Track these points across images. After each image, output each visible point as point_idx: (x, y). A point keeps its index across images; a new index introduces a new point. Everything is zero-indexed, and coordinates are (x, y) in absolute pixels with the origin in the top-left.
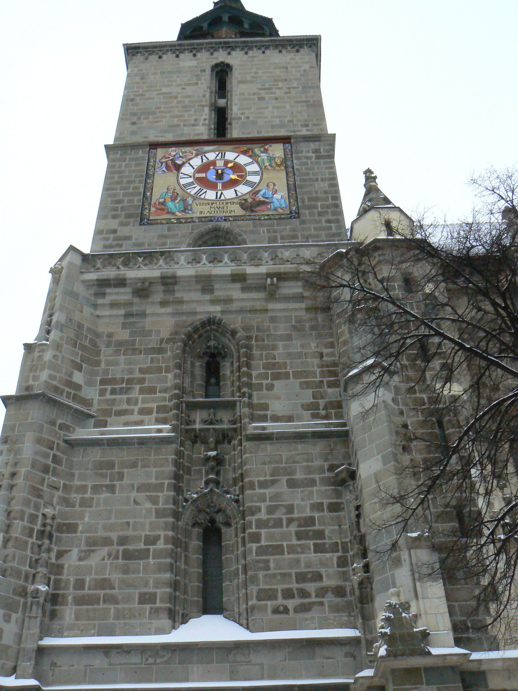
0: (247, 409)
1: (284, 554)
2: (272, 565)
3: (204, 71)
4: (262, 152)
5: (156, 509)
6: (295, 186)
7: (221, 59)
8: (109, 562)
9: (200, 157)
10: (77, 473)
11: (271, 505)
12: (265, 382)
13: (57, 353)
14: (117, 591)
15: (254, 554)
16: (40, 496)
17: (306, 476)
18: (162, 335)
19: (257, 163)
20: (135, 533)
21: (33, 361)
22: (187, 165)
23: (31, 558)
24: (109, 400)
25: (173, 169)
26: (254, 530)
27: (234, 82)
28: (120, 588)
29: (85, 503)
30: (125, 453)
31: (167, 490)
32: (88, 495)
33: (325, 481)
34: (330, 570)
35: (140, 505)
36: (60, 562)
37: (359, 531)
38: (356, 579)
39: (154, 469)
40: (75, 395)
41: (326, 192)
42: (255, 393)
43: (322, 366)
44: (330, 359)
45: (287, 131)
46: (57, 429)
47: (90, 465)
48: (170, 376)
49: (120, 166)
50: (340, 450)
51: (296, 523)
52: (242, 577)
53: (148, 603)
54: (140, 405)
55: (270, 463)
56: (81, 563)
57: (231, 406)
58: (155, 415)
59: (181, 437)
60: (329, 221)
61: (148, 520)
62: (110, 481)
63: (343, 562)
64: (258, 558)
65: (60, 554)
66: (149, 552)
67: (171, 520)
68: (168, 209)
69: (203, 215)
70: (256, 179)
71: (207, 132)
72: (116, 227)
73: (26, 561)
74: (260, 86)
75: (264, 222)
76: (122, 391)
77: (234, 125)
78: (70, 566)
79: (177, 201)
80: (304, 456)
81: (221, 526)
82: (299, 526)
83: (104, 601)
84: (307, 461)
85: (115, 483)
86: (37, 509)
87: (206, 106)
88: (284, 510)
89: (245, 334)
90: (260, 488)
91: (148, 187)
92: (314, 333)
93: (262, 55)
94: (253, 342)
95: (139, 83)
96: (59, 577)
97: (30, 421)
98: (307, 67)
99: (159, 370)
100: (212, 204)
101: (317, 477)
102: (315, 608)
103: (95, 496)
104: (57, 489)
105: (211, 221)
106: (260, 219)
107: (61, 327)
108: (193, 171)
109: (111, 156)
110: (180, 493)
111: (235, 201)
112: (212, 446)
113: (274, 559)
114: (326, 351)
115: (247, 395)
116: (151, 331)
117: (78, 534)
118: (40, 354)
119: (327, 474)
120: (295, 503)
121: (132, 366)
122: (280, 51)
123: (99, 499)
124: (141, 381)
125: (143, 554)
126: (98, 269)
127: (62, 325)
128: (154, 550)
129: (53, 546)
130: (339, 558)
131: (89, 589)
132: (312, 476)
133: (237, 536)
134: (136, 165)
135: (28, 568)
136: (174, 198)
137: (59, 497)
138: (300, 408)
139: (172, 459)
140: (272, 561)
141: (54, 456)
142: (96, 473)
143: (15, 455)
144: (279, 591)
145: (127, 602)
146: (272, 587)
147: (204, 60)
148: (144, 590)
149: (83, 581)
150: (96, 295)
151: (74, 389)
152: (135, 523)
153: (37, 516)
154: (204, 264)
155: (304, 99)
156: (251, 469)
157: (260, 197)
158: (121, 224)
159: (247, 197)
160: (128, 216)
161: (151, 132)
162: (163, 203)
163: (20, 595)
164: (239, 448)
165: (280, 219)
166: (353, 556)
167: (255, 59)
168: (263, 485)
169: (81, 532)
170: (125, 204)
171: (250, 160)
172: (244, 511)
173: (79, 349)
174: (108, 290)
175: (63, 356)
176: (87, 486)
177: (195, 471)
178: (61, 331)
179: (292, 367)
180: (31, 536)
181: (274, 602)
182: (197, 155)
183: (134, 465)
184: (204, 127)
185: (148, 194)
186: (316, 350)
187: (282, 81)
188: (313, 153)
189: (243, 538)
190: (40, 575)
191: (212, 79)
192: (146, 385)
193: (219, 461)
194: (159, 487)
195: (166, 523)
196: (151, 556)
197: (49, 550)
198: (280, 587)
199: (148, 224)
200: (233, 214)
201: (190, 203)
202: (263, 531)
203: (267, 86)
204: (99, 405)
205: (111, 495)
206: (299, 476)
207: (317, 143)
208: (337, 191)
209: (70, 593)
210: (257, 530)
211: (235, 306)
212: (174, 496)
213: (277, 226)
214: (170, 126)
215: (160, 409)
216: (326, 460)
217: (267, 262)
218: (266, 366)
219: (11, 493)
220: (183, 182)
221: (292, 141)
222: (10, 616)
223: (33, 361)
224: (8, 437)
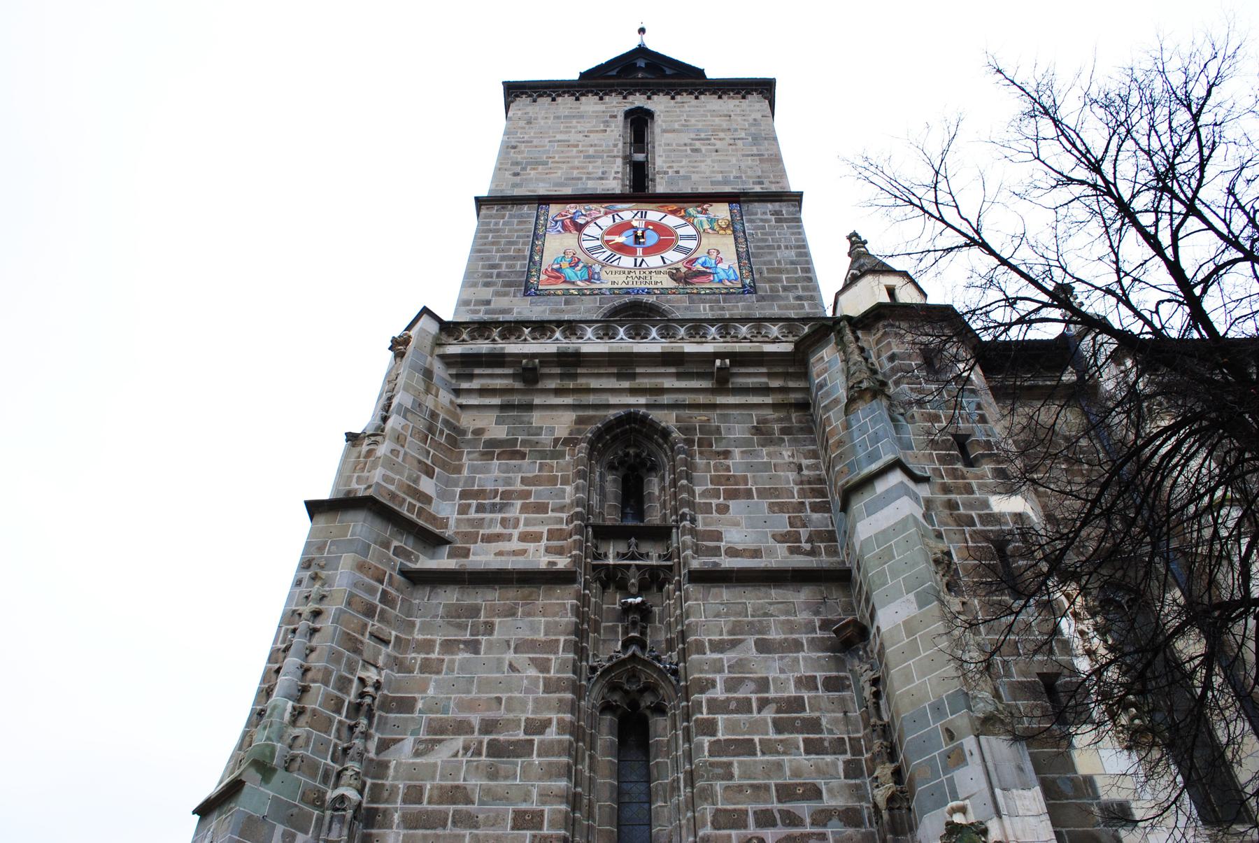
0: (689, 537)
1: (755, 754)
2: (736, 771)
3: (615, 117)
4: (698, 212)
5: (545, 678)
6: (748, 254)
7: (637, 104)
8: (465, 759)
9: (610, 216)
10: (418, 621)
11: (732, 678)
12: (714, 502)
13: (399, 448)
14: (476, 806)
15: (706, 753)
16: (357, 651)
17: (787, 636)
18: (556, 435)
19: (693, 224)
20: (511, 716)
21: (359, 457)
22: (592, 225)
23: (336, 746)
24: (474, 519)
25: (572, 228)
27: (657, 130)
28: (482, 803)
29: (427, 667)
30: (497, 595)
31: (563, 651)
32: (434, 656)
33: (816, 644)
34: (834, 782)
35: (519, 672)
36: (383, 757)
37: (881, 718)
38: (881, 795)
39: (543, 619)
40: (421, 511)
41: (792, 263)
42: (700, 517)
43: (802, 483)
44: (812, 473)
46: (391, 554)
47: (441, 611)
48: (568, 489)
49: (496, 224)
50: (837, 598)
51: (774, 706)
52: (684, 792)
53: (528, 829)
54: (521, 528)
55: (727, 615)
56: (418, 760)
58: (544, 542)
59: (585, 575)
60: (799, 298)
61: (531, 696)
62: (472, 635)
63: (852, 770)
64: (712, 759)
65: (384, 746)
66: (533, 745)
67: (569, 696)
68: (565, 277)
69: (616, 286)
70: (692, 244)
71: (620, 187)
73: (327, 751)
74: (693, 136)
75: (704, 297)
76: (494, 508)
77: (658, 180)
78: (398, 764)
79: (579, 268)
80: (780, 606)
81: (648, 713)
82: (778, 711)
83: (454, 823)
84: (787, 613)
85: (480, 637)
86: (352, 670)
87: (618, 157)
88: (752, 686)
89: (683, 437)
90: (712, 651)
92: (786, 437)
93: (694, 102)
94: (696, 448)
95: (524, 128)
96: (380, 782)
97: (349, 537)
98: (758, 116)
99: (552, 481)
100: (629, 273)
101: (804, 638)
103: (447, 658)
104: (386, 643)
105: (628, 293)
106: (698, 294)
107: (405, 412)
108: (601, 232)
109: (483, 212)
110: (584, 658)
111: (662, 270)
112: (634, 590)
113: (740, 763)
114: (805, 462)
115: (688, 518)
116: (541, 428)
117: (416, 715)
118: (372, 447)
119: (819, 634)
120: (771, 676)
121: (510, 475)
122: (720, 97)
123: (452, 661)
124: (527, 494)
125: (523, 749)
126: (463, 340)
127: (407, 410)
128: (541, 743)
129: (372, 731)
130: (847, 763)
131: (429, 803)
132: (795, 636)
133: (674, 727)
134: (520, 223)
135: (329, 761)
136: (574, 265)
137: (388, 656)
138: (771, 540)
139: (572, 606)
140: (736, 765)
141: (384, 592)
142: (448, 623)
143: (323, 585)
144: (750, 814)
145: (493, 825)
146: (739, 807)
147: (615, 104)
148: (523, 806)
149: (420, 790)
150: (458, 376)
151: (419, 500)
152: (509, 699)
153: (351, 681)
154: (622, 339)
155: (755, 152)
156: (697, 623)
157: (698, 266)
158: (497, 294)
159: (680, 265)
160: (508, 284)
161: (541, 185)
162: (559, 270)
163: (313, 803)
164: (677, 593)
166: (873, 759)
167: (686, 105)
168: (718, 647)
169: (420, 712)
170: (504, 269)
171: (683, 222)
172: (686, 687)
173: (430, 446)
174: (477, 371)
175: (406, 453)
176: (434, 641)
177: (605, 628)
178: (405, 417)
179: (755, 483)
180: (339, 712)
181: (743, 831)
182: (606, 214)
183: (512, 613)
184: (615, 182)
185: (537, 258)
186: (791, 459)
187: (723, 130)
188: (772, 215)
189: (687, 731)
190: (349, 773)
191: (625, 127)
192: (532, 500)
193: (644, 612)
194: (551, 646)
195: (560, 700)
196: (535, 752)
197: (366, 736)
198: (751, 808)
199: (537, 295)
200: (659, 286)
201: (597, 270)
202: (720, 718)
203: (703, 136)
204: (457, 527)
205: (473, 656)
206: (774, 635)
207: (777, 204)
208: (809, 262)
209: (397, 809)
210: (711, 716)
211: (666, 399)
212: (574, 660)
213: (724, 302)
214: (567, 179)
215: (552, 535)
216: (817, 613)
217: (714, 339)
218: (716, 480)
219: (310, 640)
220: (586, 245)
222: (293, 836)
223: (359, 457)
224: (314, 559)
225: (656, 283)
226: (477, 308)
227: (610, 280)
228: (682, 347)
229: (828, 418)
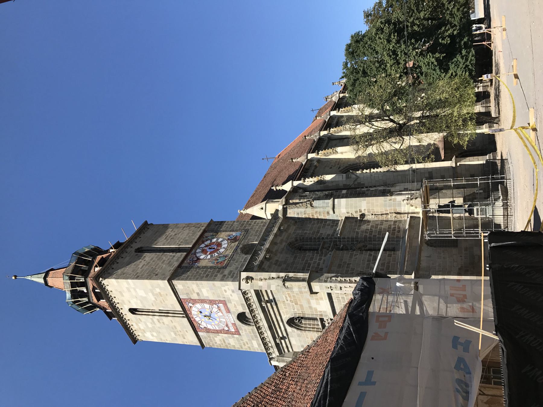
26: (372, 236)
43: (318, 224)
45: (198, 232)
57: (324, 243)
70: (220, 240)
72: (222, 275)
91: (206, 267)
102: (400, 226)
105: (236, 250)
114: (312, 223)
119: (358, 223)
148: (387, 256)
160: (218, 272)
162: (217, 263)
165: (246, 234)
174: (263, 267)
182: (195, 254)
195: (365, 252)
199: (227, 266)
200: (236, 245)
221: (207, 230)
225: (235, 245)
226: (226, 277)
227: (230, 253)
228: (274, 233)
229: (308, 214)
